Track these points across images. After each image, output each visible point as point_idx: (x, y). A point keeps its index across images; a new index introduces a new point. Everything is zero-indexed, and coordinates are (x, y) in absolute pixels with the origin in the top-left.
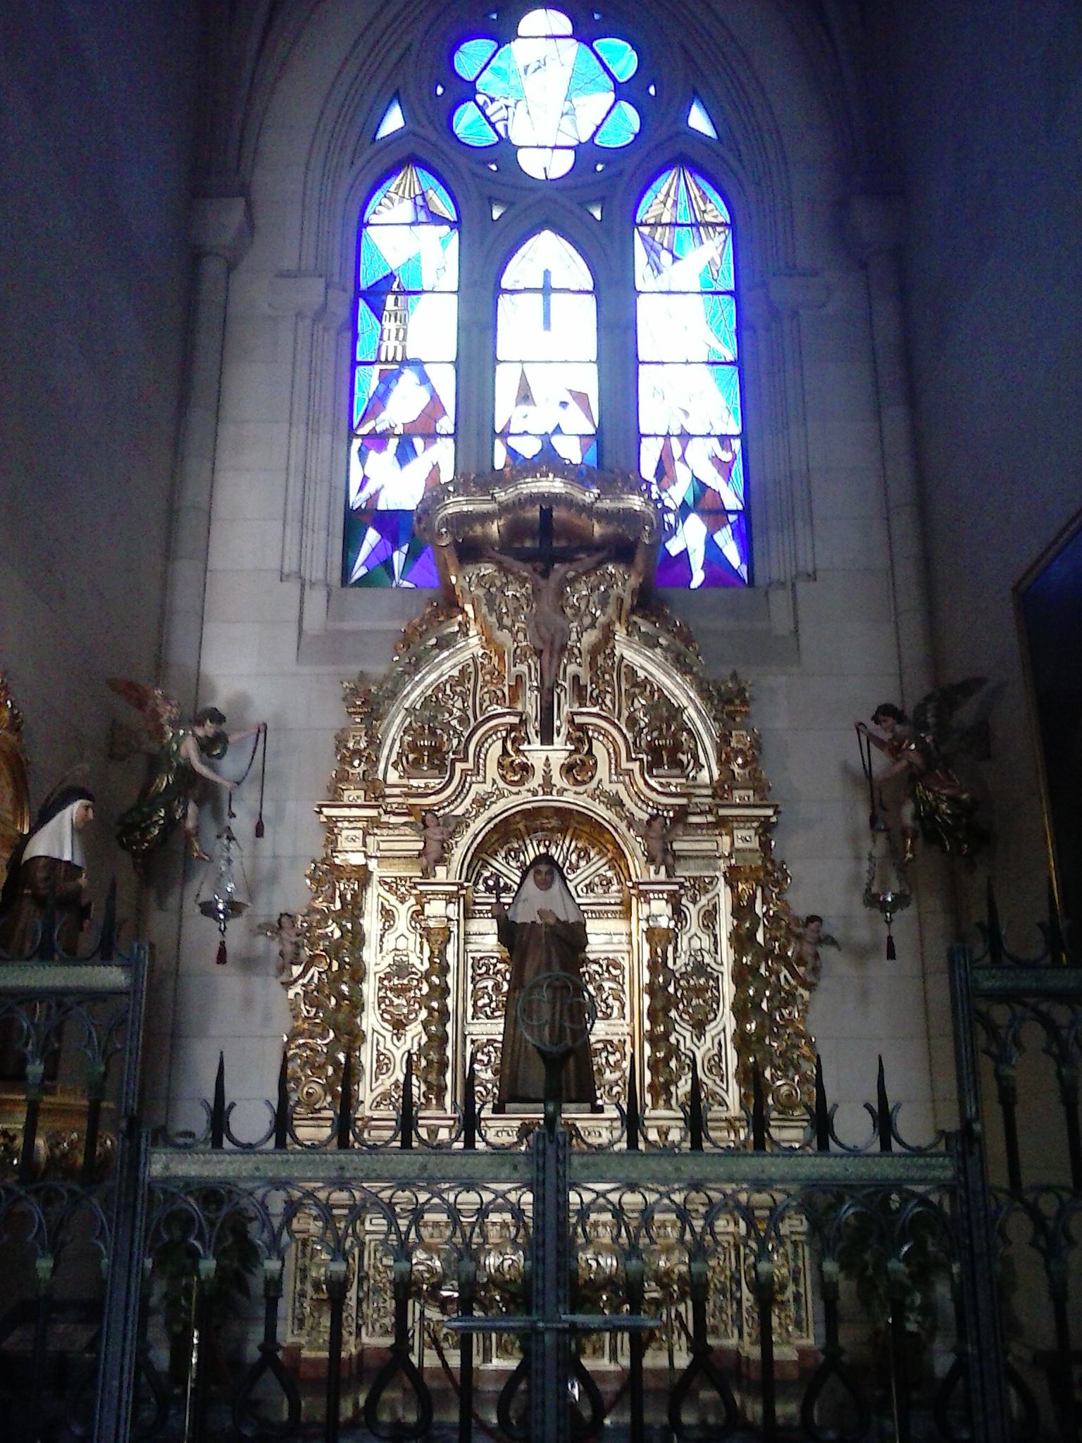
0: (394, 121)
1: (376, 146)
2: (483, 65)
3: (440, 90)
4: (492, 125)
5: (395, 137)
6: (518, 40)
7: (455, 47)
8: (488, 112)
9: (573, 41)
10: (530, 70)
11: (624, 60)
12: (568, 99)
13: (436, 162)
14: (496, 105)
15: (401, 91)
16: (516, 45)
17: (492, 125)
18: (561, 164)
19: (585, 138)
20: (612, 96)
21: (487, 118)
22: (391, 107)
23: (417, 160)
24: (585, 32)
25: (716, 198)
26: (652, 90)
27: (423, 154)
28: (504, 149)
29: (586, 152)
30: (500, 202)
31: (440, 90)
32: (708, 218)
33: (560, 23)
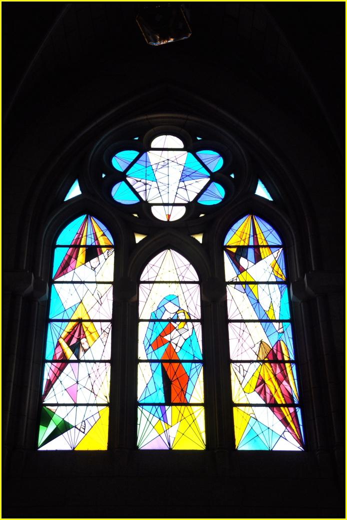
0: (75, 191)
4: (137, 194)
10: (159, 167)
11: (216, 162)
12: (182, 180)
16: (150, 154)
18: (178, 213)
20: (207, 180)
28: (144, 207)
29: (193, 207)
33: (177, 142)
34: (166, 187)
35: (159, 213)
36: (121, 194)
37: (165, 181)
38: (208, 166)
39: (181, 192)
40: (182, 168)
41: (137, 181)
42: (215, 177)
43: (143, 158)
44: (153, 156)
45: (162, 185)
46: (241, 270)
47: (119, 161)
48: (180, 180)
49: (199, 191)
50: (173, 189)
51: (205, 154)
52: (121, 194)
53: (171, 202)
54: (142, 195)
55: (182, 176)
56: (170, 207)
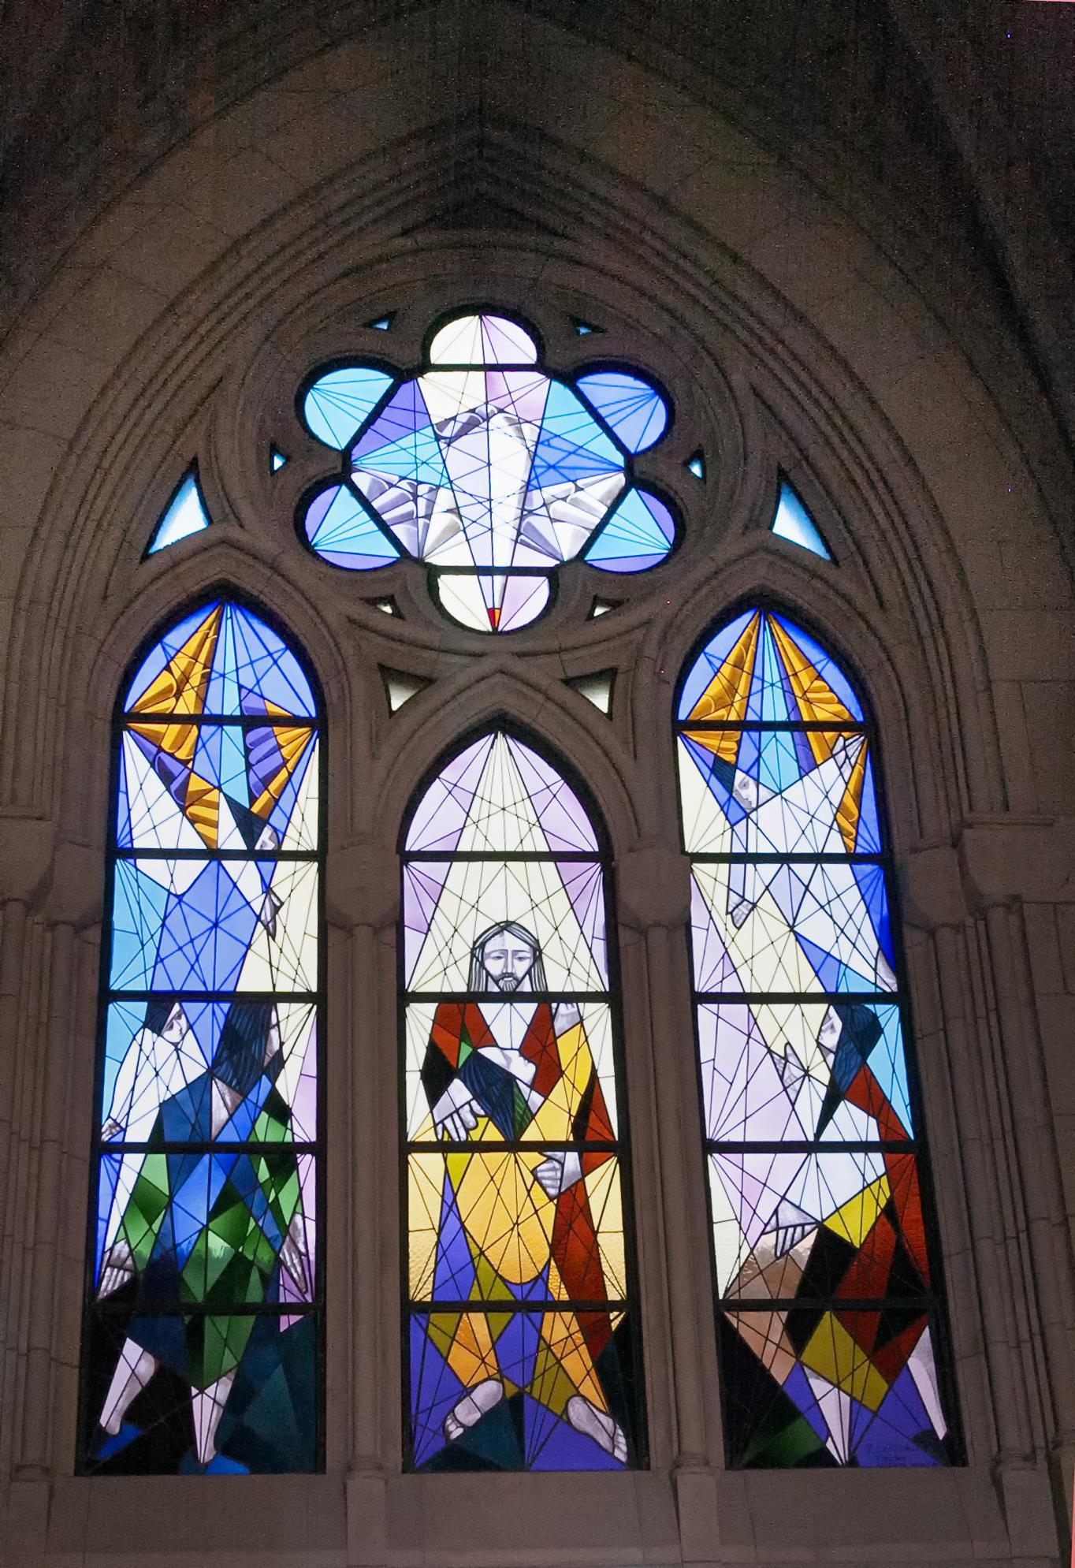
1: (152, 566)
2: (363, 417)
3: (278, 463)
5: (192, 548)
6: (430, 375)
7: (309, 381)
8: (376, 504)
9: (536, 376)
13: (275, 602)
14: (392, 494)
15: (202, 465)
16: (429, 383)
17: (385, 528)
19: (568, 551)
20: (620, 479)
21: (375, 516)
22: (183, 489)
23: (512, 723)
24: (559, 359)
25: (832, 672)
26: (696, 469)
27: (251, 581)
30: (404, 678)
31: (278, 463)
32: (822, 715)
34: (483, 510)
37: (476, 484)
38: (618, 431)
40: (530, 432)
41: (391, 485)
43: (406, 389)
45: (472, 500)
46: (737, 813)
48: (528, 483)
50: (506, 513)
51: (606, 388)
53: (502, 561)
55: (533, 467)
56: (499, 580)
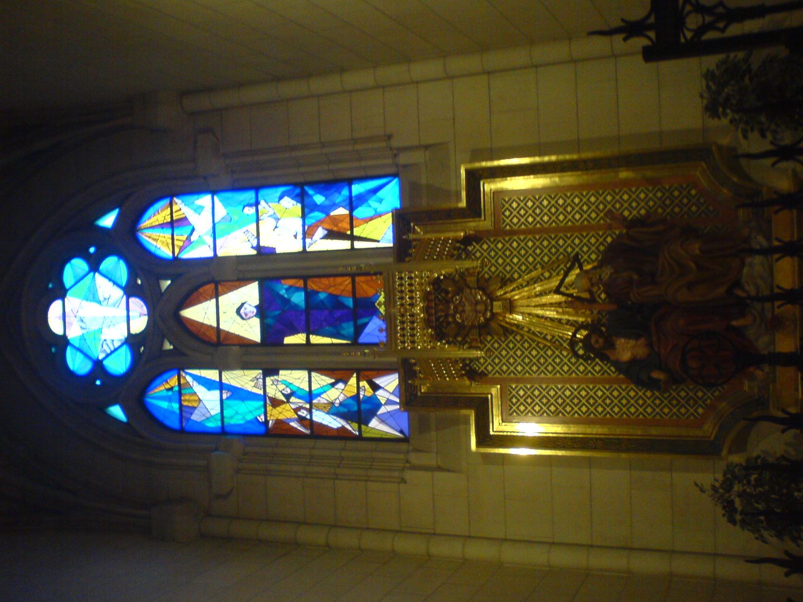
0: (116, 411)
10: (84, 326)
18: (138, 306)
20: (97, 274)
28: (132, 341)
29: (130, 290)
35: (139, 324)
36: (119, 364)
39: (111, 301)
42: (94, 267)
43: (71, 342)
44: (73, 334)
47: (77, 363)
49: (111, 284)
52: (119, 364)
54: (117, 344)
